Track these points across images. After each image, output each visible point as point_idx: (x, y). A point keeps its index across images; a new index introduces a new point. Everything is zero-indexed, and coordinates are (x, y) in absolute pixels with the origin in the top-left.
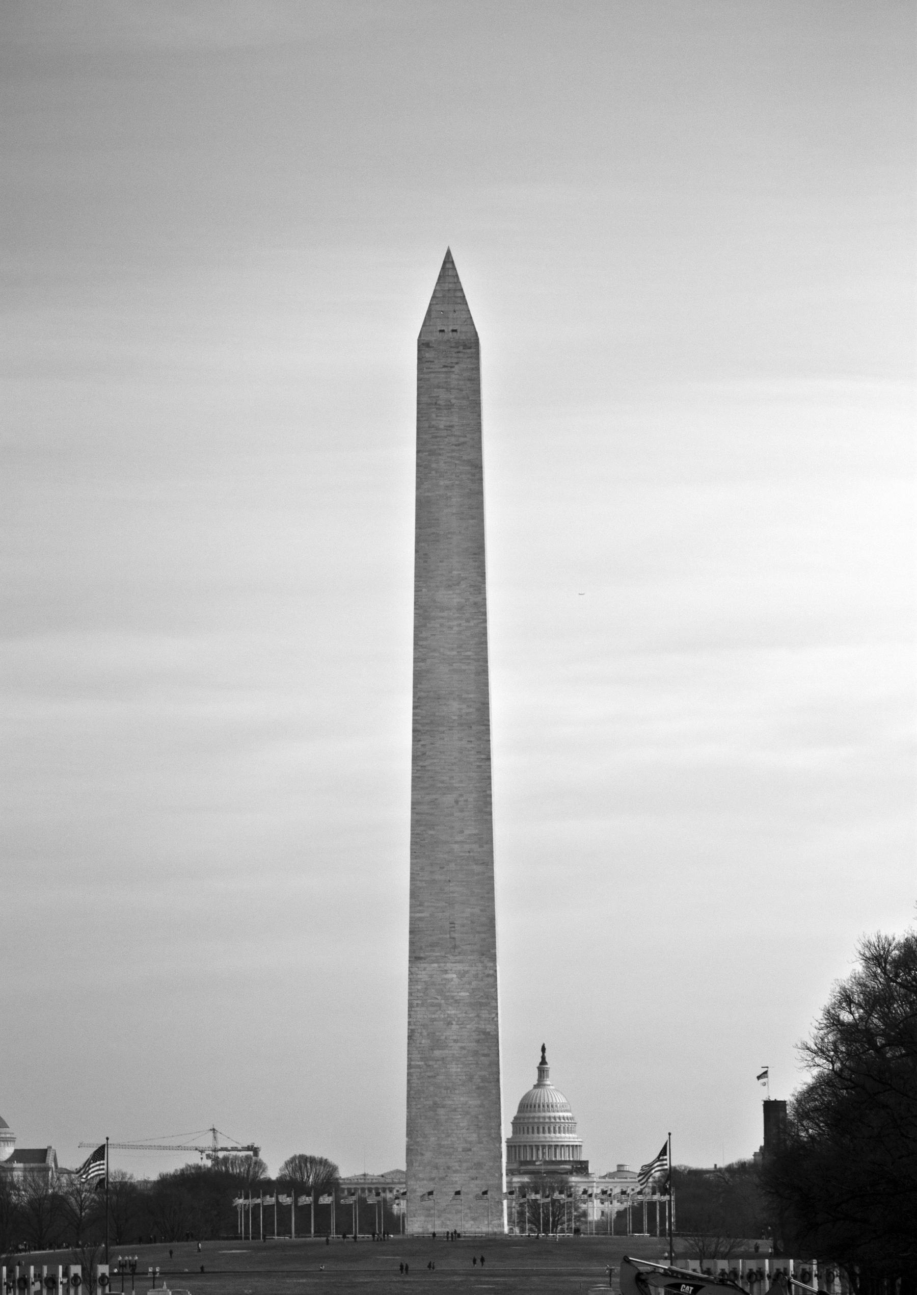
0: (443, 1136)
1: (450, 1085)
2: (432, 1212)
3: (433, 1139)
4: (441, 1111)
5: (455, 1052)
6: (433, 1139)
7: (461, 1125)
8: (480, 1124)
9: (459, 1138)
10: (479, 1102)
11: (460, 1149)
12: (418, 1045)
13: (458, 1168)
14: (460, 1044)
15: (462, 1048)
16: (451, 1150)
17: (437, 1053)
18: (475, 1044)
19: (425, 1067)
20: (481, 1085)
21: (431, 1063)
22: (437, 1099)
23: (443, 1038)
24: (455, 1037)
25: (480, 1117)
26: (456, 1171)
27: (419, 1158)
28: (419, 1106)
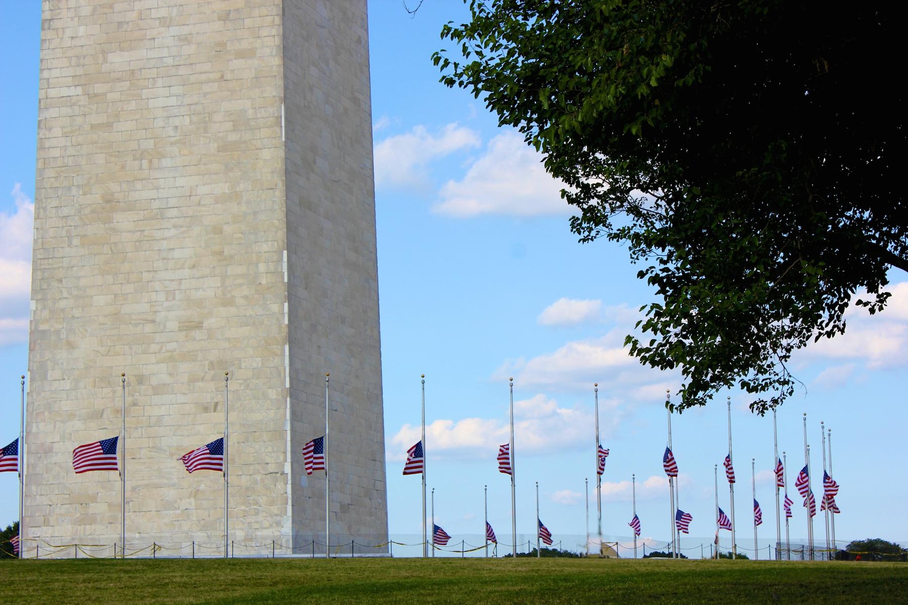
0: (129, 288)
1: (149, 145)
2: (94, 508)
3: (100, 300)
4: (123, 221)
5: (165, 52)
6: (100, 300)
7: (177, 254)
8: (227, 251)
9: (171, 295)
10: (222, 188)
11: (172, 325)
12: (68, 43)
13: (166, 379)
14: (174, 30)
15: (185, 40)
16: (149, 328)
17: (118, 60)
18: (218, 25)
19: (84, 100)
20: (233, 137)
21: (99, 88)
22: (114, 187)
23: (133, 16)
24: (163, 13)
25: (226, 228)
26: (158, 390)
27: (62, 354)
28: (65, 211)
